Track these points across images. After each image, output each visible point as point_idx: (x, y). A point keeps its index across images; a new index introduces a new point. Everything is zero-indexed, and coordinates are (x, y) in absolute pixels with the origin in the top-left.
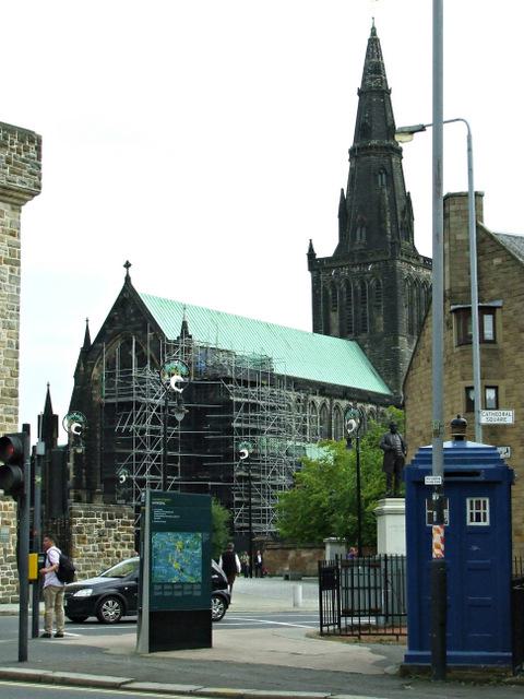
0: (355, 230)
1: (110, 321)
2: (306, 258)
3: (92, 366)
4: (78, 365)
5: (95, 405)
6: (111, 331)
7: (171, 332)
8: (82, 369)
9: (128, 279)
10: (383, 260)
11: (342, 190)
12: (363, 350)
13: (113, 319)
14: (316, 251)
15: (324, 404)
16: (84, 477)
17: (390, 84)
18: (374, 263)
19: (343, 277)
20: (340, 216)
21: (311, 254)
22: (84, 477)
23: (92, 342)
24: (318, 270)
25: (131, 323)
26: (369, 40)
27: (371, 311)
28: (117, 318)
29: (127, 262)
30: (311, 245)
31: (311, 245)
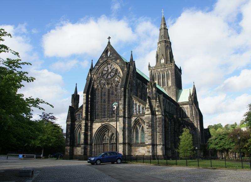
0: (161, 60)
4: (88, 75)
6: (102, 61)
8: (90, 75)
9: (109, 43)
13: (103, 56)
16: (89, 116)
18: (168, 67)
21: (149, 66)
22: (89, 116)
23: (93, 67)
27: (167, 80)
29: (109, 37)
30: (149, 65)
31: (149, 65)
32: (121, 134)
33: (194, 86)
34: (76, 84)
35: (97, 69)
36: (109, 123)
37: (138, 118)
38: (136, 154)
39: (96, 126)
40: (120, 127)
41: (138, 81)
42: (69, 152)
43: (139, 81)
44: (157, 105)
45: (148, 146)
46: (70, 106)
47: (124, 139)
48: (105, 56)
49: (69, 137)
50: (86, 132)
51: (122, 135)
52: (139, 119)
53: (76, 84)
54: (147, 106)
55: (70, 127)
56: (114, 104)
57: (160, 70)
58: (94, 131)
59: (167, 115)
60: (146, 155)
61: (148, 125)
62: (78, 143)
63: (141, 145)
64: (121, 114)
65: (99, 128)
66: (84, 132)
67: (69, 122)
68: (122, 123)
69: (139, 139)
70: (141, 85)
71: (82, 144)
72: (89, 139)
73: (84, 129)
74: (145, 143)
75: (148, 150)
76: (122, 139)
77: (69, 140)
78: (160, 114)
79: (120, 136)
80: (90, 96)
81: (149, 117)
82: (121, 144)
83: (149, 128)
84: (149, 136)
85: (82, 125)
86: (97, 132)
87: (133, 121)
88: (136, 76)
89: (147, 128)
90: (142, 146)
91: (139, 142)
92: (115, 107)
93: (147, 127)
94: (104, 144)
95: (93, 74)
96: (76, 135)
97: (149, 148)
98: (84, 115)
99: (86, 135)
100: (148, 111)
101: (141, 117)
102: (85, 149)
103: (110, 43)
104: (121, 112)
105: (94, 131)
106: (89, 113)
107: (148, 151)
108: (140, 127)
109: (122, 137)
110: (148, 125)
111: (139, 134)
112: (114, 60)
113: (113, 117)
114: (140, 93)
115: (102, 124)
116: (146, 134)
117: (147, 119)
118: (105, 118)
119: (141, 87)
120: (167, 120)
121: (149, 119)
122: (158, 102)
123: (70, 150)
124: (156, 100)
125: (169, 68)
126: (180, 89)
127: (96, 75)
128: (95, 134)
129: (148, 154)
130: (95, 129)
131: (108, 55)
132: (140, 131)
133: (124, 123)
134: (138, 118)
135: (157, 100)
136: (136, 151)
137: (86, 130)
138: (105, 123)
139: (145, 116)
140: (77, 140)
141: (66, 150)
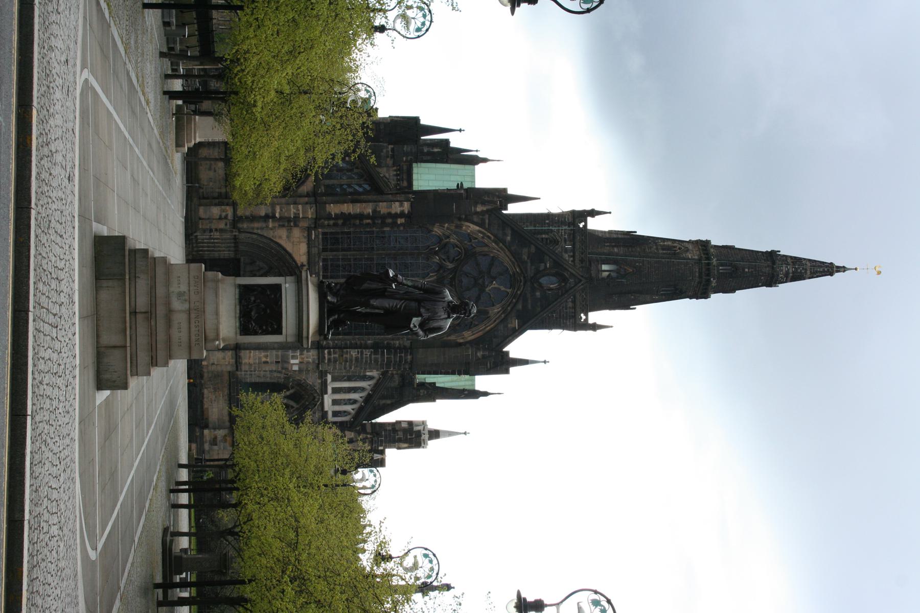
2: (588, 208)
3: (481, 225)
6: (525, 257)
7: (514, 349)
10: (575, 313)
16: (331, 222)
21: (593, 213)
28: (542, 267)
32: (266, 356)
33: (486, 394)
34: (460, 130)
38: (206, 391)
39: (300, 242)
45: (229, 439)
53: (460, 130)
58: (280, 237)
64: (329, 353)
65: (290, 255)
66: (277, 215)
75: (219, 438)
94: (239, 260)
95: (483, 221)
97: (225, 441)
98: (334, 209)
107: (215, 438)
112: (520, 306)
115: (303, 265)
118: (325, 268)
125: (570, 304)
130: (288, 237)
134: (316, 395)
136: (215, 390)
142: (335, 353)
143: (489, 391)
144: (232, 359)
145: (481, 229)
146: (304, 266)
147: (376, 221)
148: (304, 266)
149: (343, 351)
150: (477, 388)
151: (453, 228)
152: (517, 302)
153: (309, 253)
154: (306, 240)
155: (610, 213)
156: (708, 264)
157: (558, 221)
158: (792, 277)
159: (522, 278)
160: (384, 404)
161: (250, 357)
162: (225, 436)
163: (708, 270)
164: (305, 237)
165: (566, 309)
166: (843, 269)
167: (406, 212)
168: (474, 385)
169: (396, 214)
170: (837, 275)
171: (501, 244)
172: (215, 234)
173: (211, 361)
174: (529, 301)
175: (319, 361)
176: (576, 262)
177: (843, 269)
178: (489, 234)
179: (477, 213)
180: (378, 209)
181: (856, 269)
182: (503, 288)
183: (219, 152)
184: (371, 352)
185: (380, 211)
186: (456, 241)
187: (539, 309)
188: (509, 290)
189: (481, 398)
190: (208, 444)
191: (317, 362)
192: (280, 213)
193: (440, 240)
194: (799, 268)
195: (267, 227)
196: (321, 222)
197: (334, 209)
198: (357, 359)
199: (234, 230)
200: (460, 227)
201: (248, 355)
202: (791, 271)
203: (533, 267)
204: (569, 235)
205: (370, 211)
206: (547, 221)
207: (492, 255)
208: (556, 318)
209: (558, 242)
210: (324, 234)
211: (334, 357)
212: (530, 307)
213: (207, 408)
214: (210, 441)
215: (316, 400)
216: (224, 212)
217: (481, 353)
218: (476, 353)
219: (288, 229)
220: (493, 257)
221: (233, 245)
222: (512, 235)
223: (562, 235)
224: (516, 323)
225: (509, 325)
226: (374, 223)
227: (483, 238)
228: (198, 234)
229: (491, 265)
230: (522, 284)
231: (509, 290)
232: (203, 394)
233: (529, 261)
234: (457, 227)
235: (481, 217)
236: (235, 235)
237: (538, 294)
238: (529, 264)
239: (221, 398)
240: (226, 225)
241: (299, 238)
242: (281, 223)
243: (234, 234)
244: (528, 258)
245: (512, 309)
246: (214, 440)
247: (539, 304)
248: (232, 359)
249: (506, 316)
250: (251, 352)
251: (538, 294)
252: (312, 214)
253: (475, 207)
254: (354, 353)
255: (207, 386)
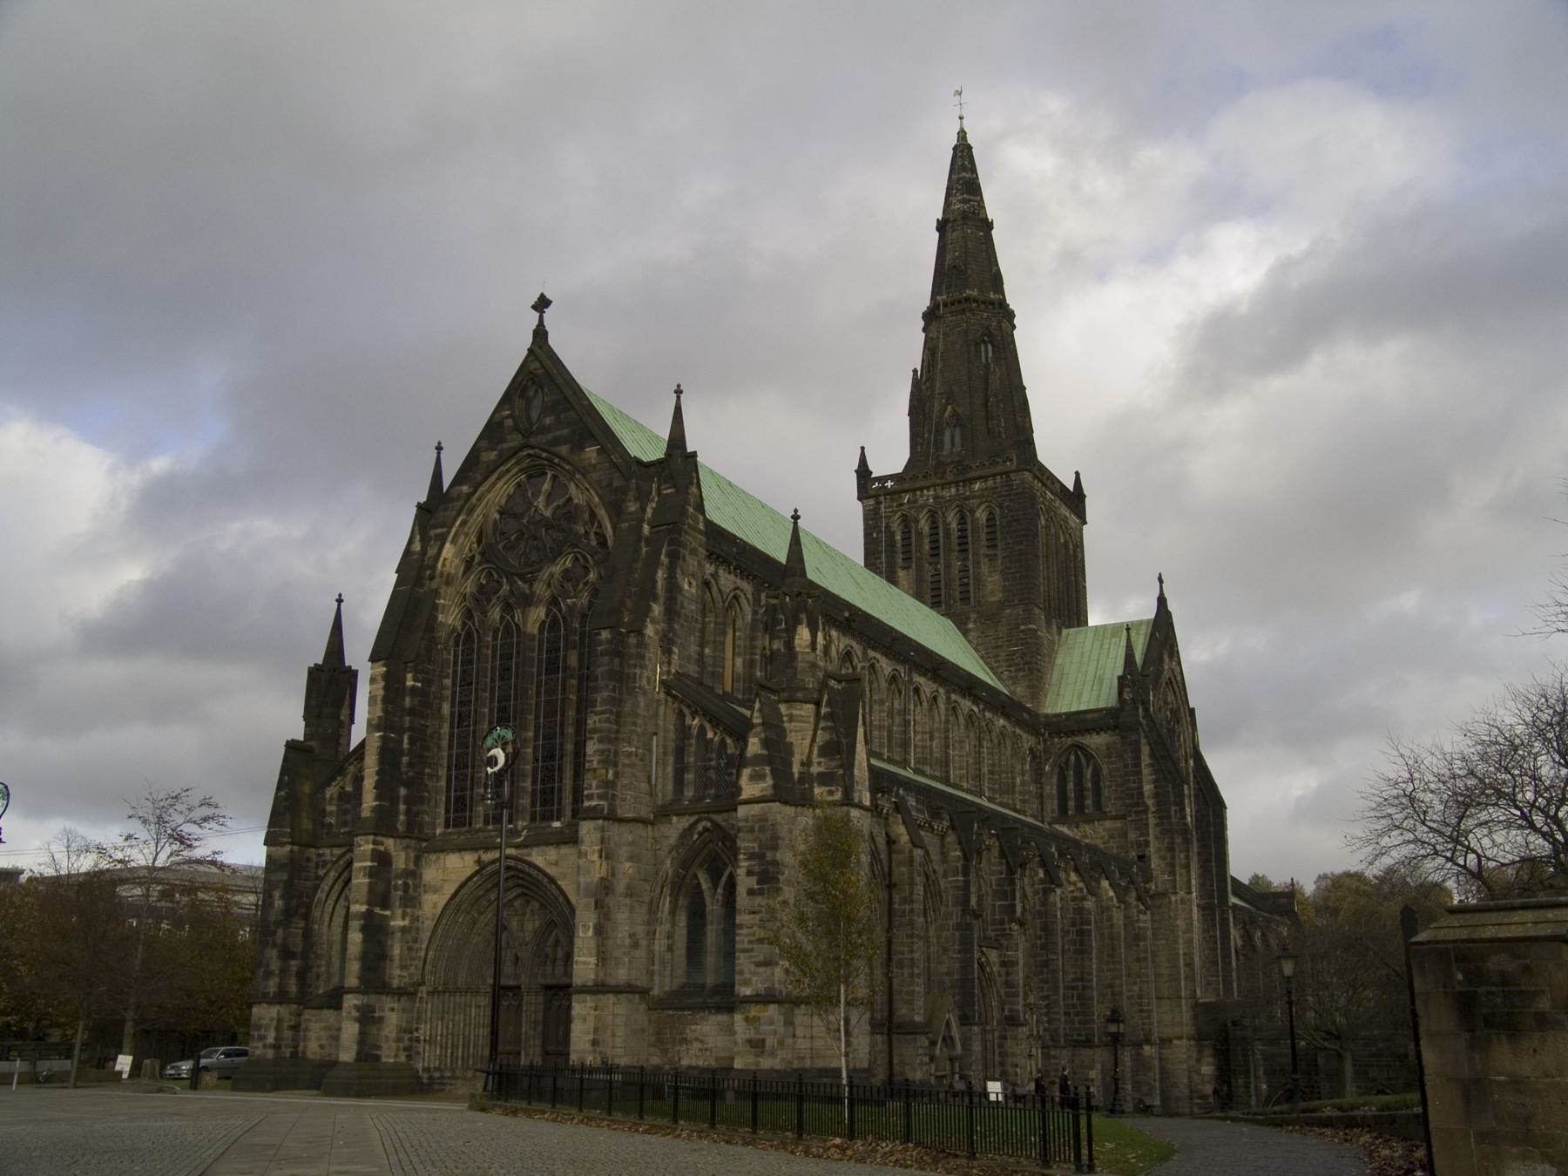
1: (492, 431)
3: (442, 540)
5: (443, 634)
6: (493, 455)
8: (417, 547)
9: (540, 334)
11: (915, 371)
12: (965, 633)
13: (501, 424)
14: (871, 468)
15: (935, 698)
16: (402, 807)
17: (992, 212)
18: (984, 478)
19: (923, 506)
20: (910, 414)
21: (863, 472)
22: (402, 807)
24: (876, 497)
25: (543, 430)
26: (955, 149)
29: (542, 297)
33: (1162, 601)
35: (460, 503)
36: (525, 851)
37: (700, 827)
38: (685, 1062)
39: (445, 869)
40: (582, 880)
41: (722, 581)
42: (271, 1040)
43: (727, 580)
44: (822, 737)
45: (754, 1011)
46: (291, 746)
47: (603, 957)
48: (509, 422)
49: (274, 945)
50: (377, 910)
51: (590, 933)
52: (706, 829)
54: (754, 746)
55: (285, 877)
56: (495, 735)
57: (935, 498)
58: (435, 906)
59: (912, 802)
60: (738, 1064)
61: (756, 869)
62: (336, 980)
63: (717, 999)
64: (590, 797)
66: (364, 908)
67: (283, 844)
68: (595, 857)
69: (711, 960)
70: (748, 609)
71: (351, 991)
72: (397, 959)
73: (365, 889)
74: (733, 985)
75: (752, 1034)
76: (593, 960)
77: (275, 965)
78: (838, 796)
79: (578, 943)
80: (409, 676)
81: (763, 819)
82: (585, 990)
83: (760, 893)
84: (760, 941)
85: (356, 865)
86: (452, 907)
87: (672, 841)
88: (702, 552)
89: (751, 892)
90: (719, 1009)
91: (710, 980)
92: (499, 754)
93: (753, 882)
95: (436, 535)
96: (325, 929)
97: (757, 1019)
98: (369, 800)
99: (375, 930)
100: (761, 777)
101: (718, 818)
102: (367, 1018)
103: (546, 333)
104: (594, 783)
105: (433, 903)
106: (403, 791)
107: (750, 1041)
108: (715, 885)
109: (593, 943)
110: (756, 869)
111: (709, 927)
112: (564, 450)
113: (552, 819)
114: (739, 661)
115: (479, 861)
116: (741, 926)
117: (752, 830)
119: (749, 618)
120: (905, 838)
121: (762, 829)
122: (830, 716)
123: (278, 1029)
124: (818, 704)
125: (990, 483)
126: (1070, 626)
127: (454, 541)
128: (436, 925)
129: (750, 1059)
130: (436, 891)
131: (535, 414)
132: (713, 907)
133: (607, 854)
134: (700, 827)
135: (824, 710)
136: (684, 1041)
137: (380, 898)
138: (495, 855)
139: (742, 811)
140: (329, 964)
141: (259, 1027)
142: (590, 787)
143: (1157, 594)
144: (585, 1002)
145: (450, 538)
146: (479, 858)
147: (407, 724)
148: (479, 858)
149: (589, 770)
150: (1152, 615)
151: (451, 590)
152: (560, 457)
153: (460, 849)
154: (442, 856)
155: (863, 448)
156: (945, 305)
157: (872, 519)
158: (969, 193)
159: (524, 454)
160: (1152, 755)
161: (585, 963)
162: (747, 1019)
163: (953, 304)
164: (438, 858)
165: (997, 488)
166: (962, 135)
167: (385, 669)
168: (1148, 621)
169: (386, 688)
170: (970, 141)
171: (474, 499)
172: (422, 1032)
173: (588, 1047)
174: (558, 433)
175: (598, 818)
176: (928, 484)
177: (962, 135)
178: (457, 524)
179: (424, 552)
180: (375, 722)
181: (961, 118)
182: (546, 486)
183: (316, 1022)
184: (592, 712)
185: (379, 717)
186: (469, 582)
187: (572, 414)
188: (549, 475)
189: (1171, 606)
190: (761, 1060)
191: (600, 822)
192: (361, 904)
193: (468, 614)
194: (957, 189)
195: (404, 930)
196: (400, 827)
197: (369, 800)
198: (601, 741)
199: (419, 995)
200: (449, 580)
201: (582, 966)
202: (960, 198)
203: (509, 437)
204: (892, 500)
205: (379, 734)
206: (875, 535)
207: (497, 516)
208: (1010, 501)
209: (903, 515)
210: (447, 825)
211: (598, 787)
212: (565, 432)
213: (717, 1059)
214: (757, 1056)
215: (709, 825)
216: (350, 1013)
217: (630, 504)
218: (631, 513)
219: (425, 892)
220: (501, 513)
221: (452, 998)
222: (461, 484)
223: (893, 511)
224: (591, 452)
225: (594, 462)
226: (411, 729)
227: (467, 535)
228: (421, 1065)
229: (515, 516)
230: (532, 452)
231: (549, 475)
232: (690, 1067)
233: (499, 447)
234: (448, 583)
235: (432, 542)
236: (428, 992)
237: (548, 421)
238: (505, 446)
239: (698, 1027)
240: (393, 1010)
241: (438, 870)
242: (398, 904)
243: (425, 995)
244: (493, 450)
245: (568, 463)
246: (755, 1047)
247: (562, 416)
248: (585, 1002)
249: (579, 472)
250: (577, 961)
251: (548, 421)
252: (367, 843)
253: (414, 553)
254: (591, 747)
255: (676, 1059)
